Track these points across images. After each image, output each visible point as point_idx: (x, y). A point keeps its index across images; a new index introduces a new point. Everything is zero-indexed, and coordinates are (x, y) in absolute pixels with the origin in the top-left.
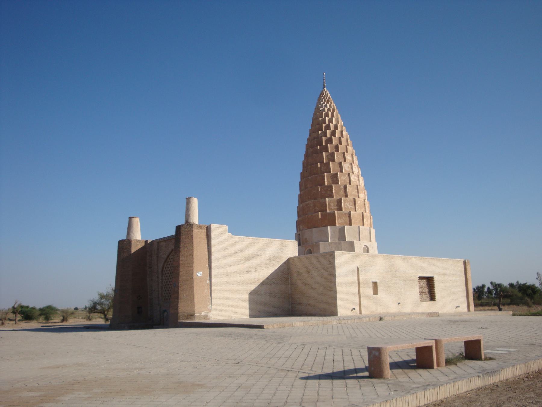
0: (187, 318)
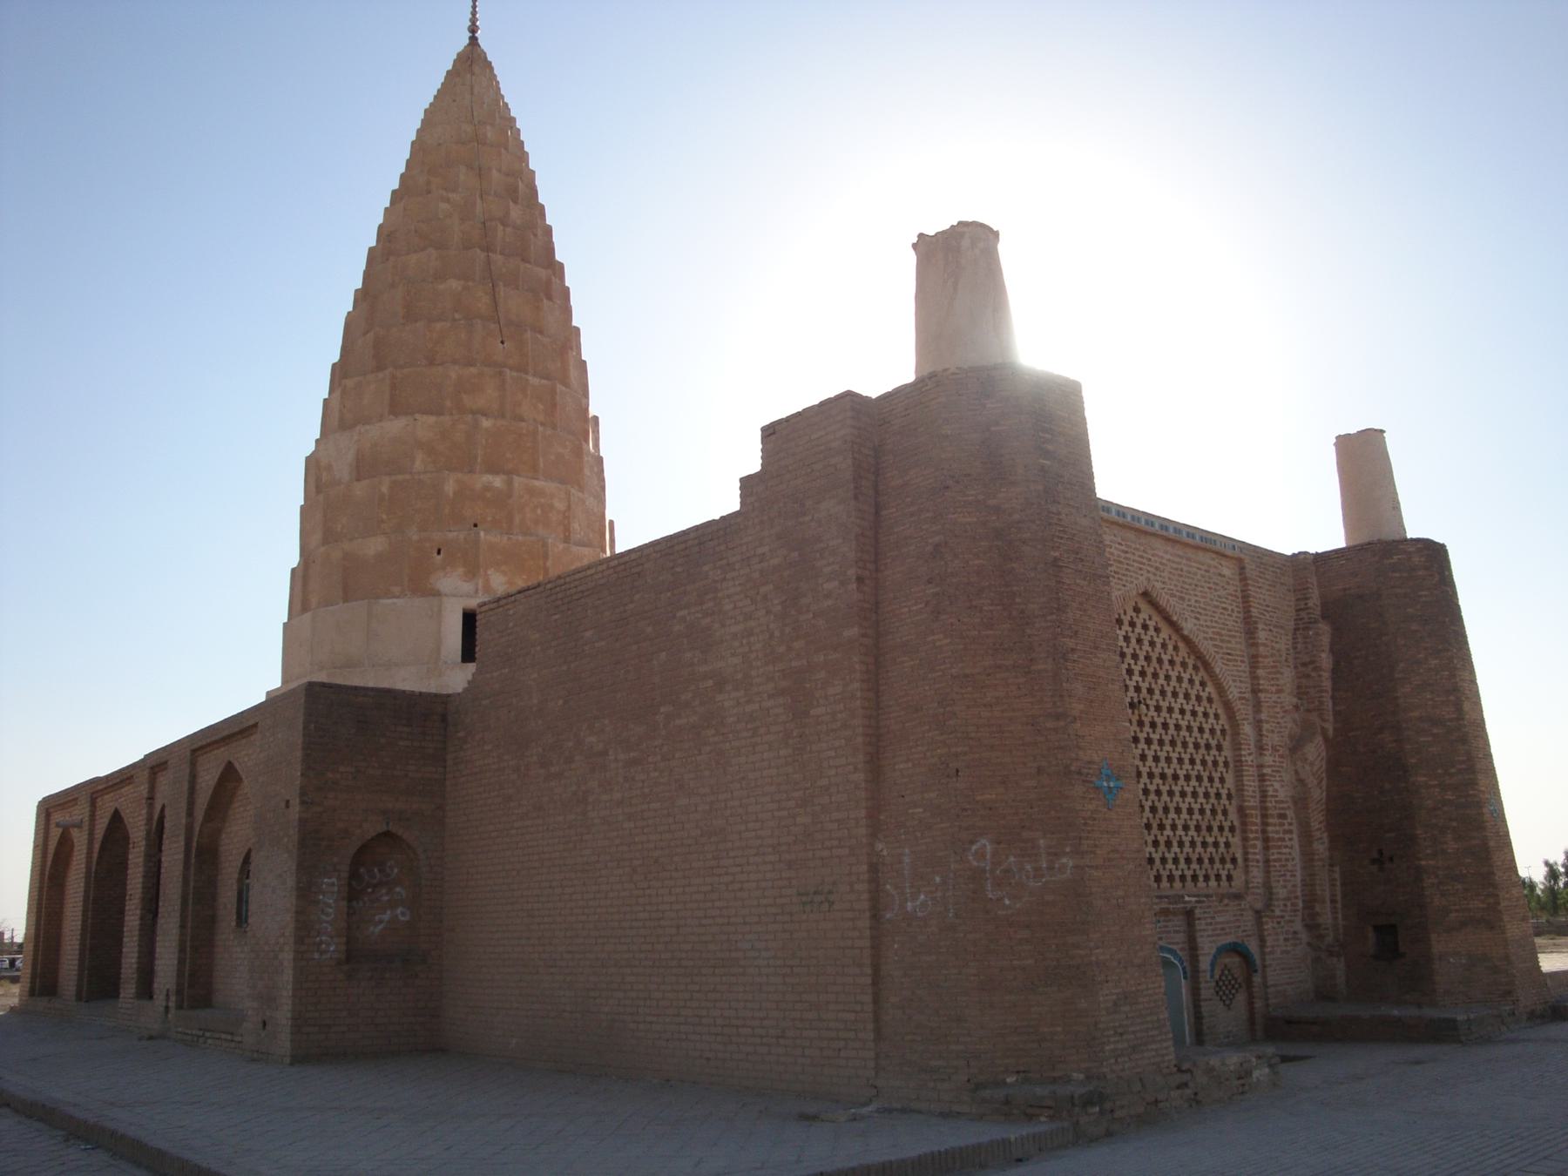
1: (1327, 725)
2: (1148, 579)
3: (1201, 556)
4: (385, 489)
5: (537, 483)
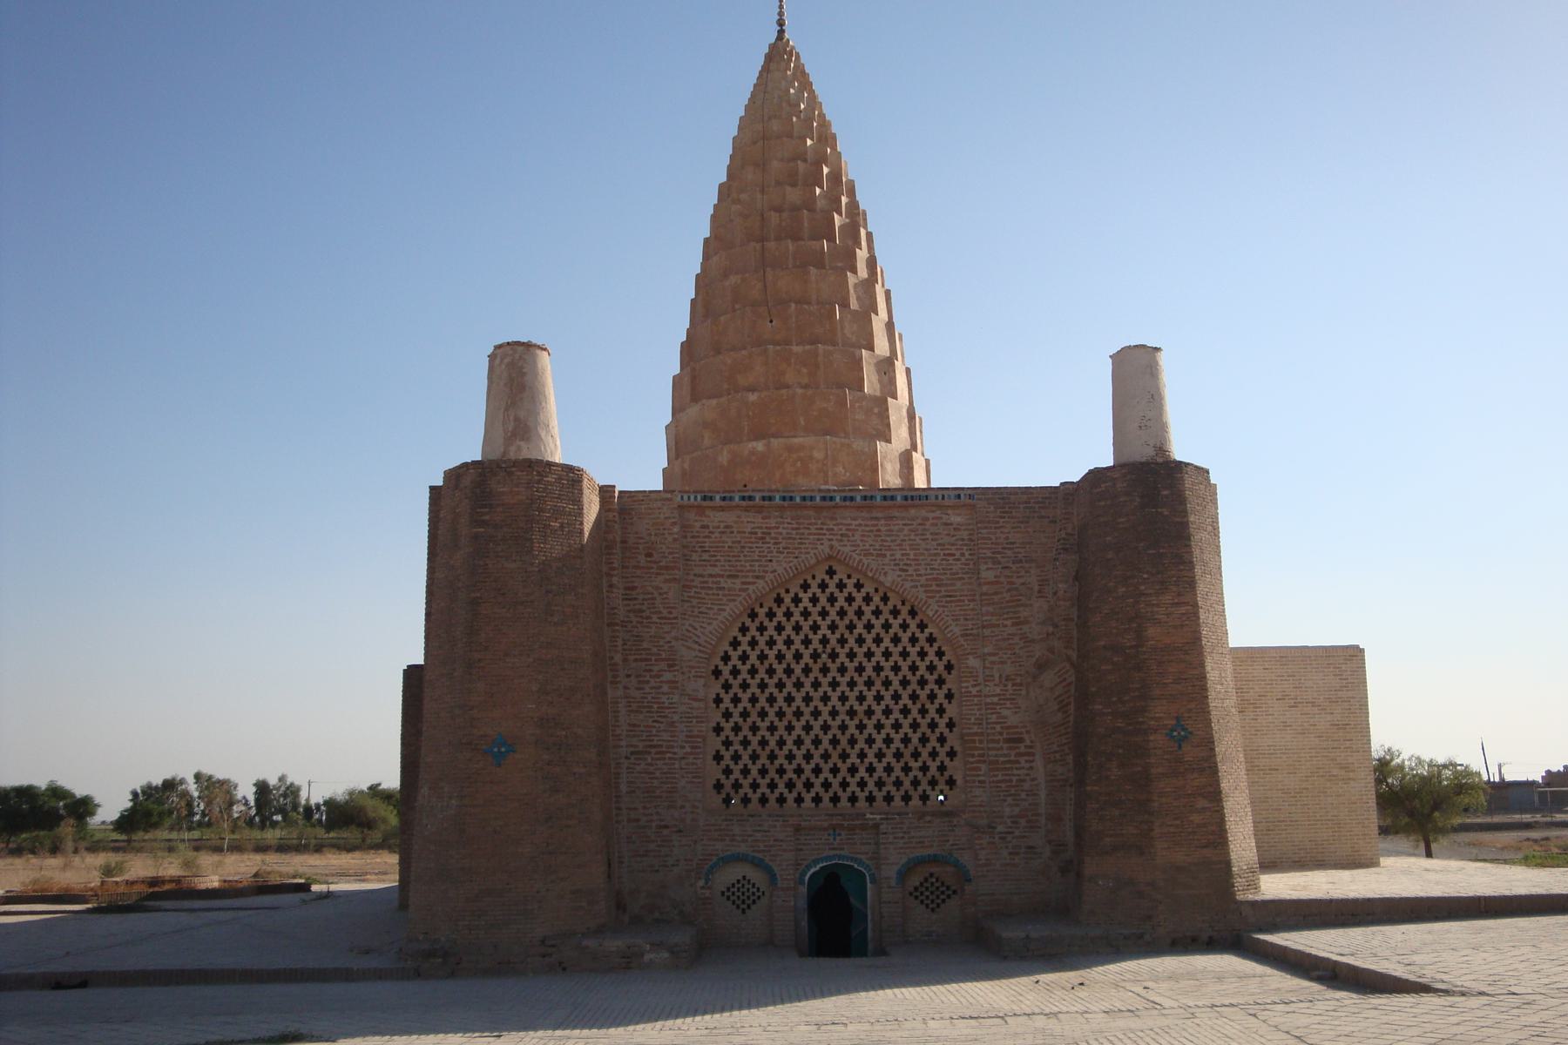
1: (1070, 652)
2: (831, 547)
3: (913, 512)
4: (686, 466)
5: (796, 440)
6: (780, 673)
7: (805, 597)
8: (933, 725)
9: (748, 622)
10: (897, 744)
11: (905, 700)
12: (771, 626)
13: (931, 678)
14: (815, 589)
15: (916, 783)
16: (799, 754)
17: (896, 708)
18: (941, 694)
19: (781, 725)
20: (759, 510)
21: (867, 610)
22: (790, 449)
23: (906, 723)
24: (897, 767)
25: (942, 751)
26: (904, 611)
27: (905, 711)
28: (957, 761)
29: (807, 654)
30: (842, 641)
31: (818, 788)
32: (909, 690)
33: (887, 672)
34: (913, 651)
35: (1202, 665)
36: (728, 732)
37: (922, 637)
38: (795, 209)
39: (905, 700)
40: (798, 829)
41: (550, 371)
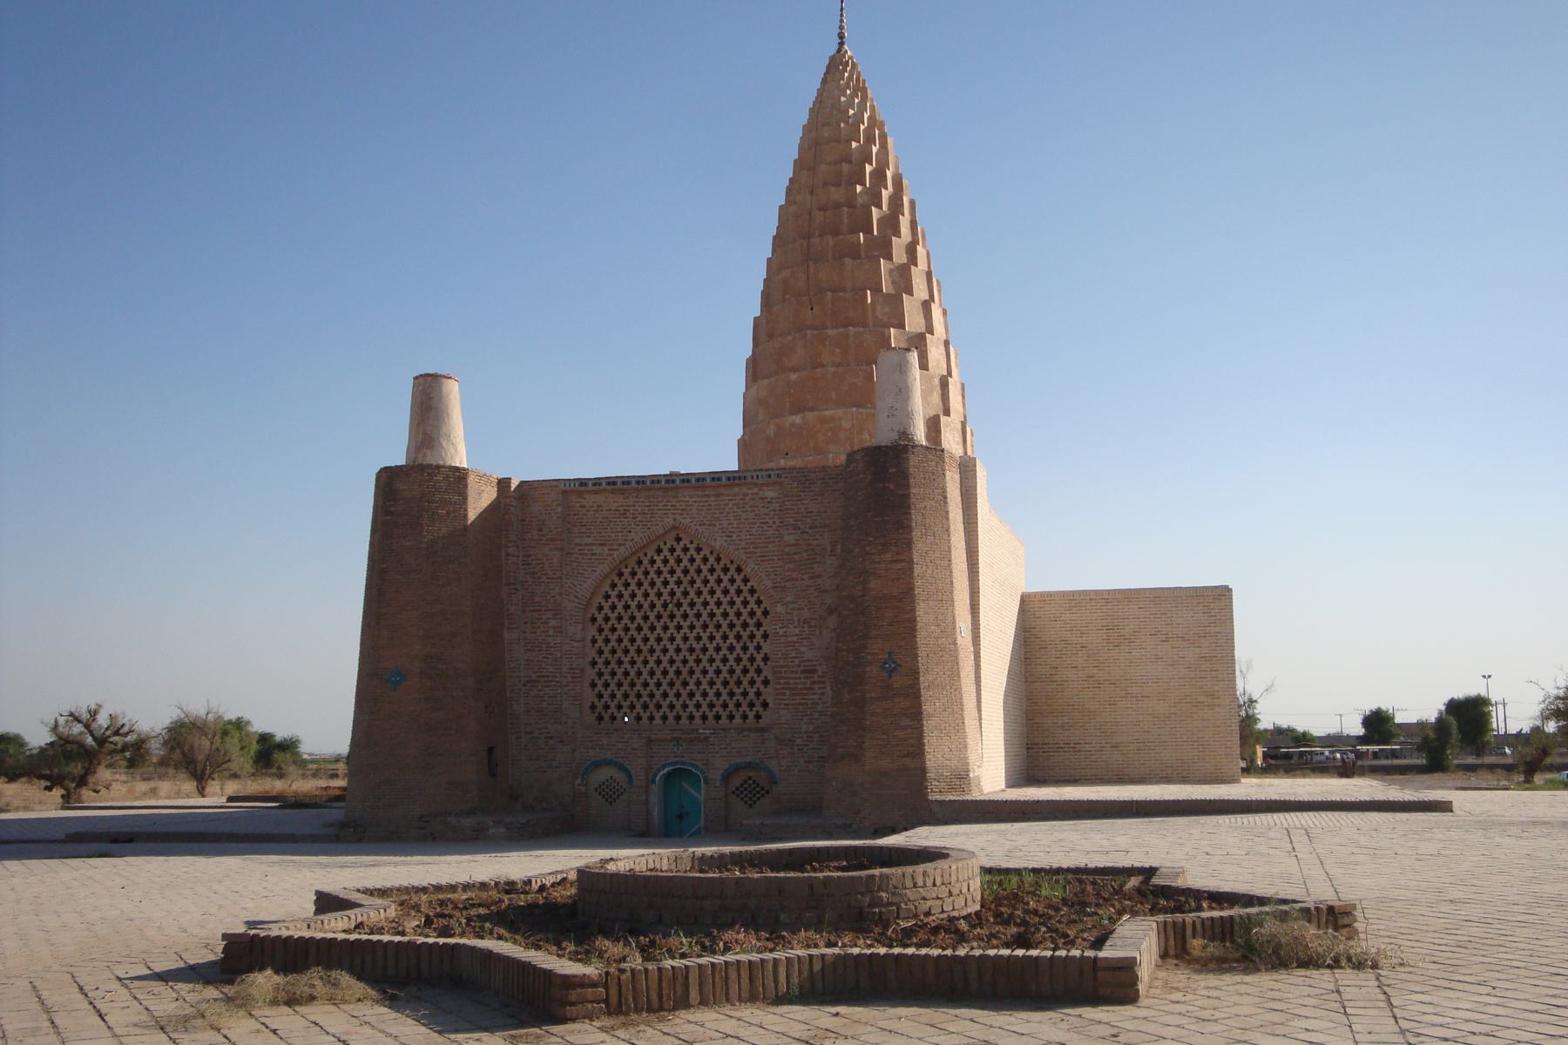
0: (952, 789)
6: (639, 620)
7: (659, 559)
8: (752, 659)
9: (616, 580)
10: (724, 674)
11: (731, 640)
12: (633, 583)
13: (751, 622)
14: (666, 552)
15: (738, 705)
16: (652, 682)
17: (724, 646)
18: (759, 635)
19: (639, 660)
20: (622, 492)
21: (705, 569)
22: (823, 421)
23: (731, 658)
24: (724, 692)
25: (759, 680)
26: (733, 568)
27: (731, 649)
28: (770, 689)
29: (659, 604)
30: (686, 594)
31: (665, 709)
32: (735, 631)
33: (719, 618)
34: (738, 600)
35: (913, 610)
36: (600, 665)
37: (745, 589)
38: (838, 206)
39: (731, 640)
40: (649, 741)
41: (453, 391)
